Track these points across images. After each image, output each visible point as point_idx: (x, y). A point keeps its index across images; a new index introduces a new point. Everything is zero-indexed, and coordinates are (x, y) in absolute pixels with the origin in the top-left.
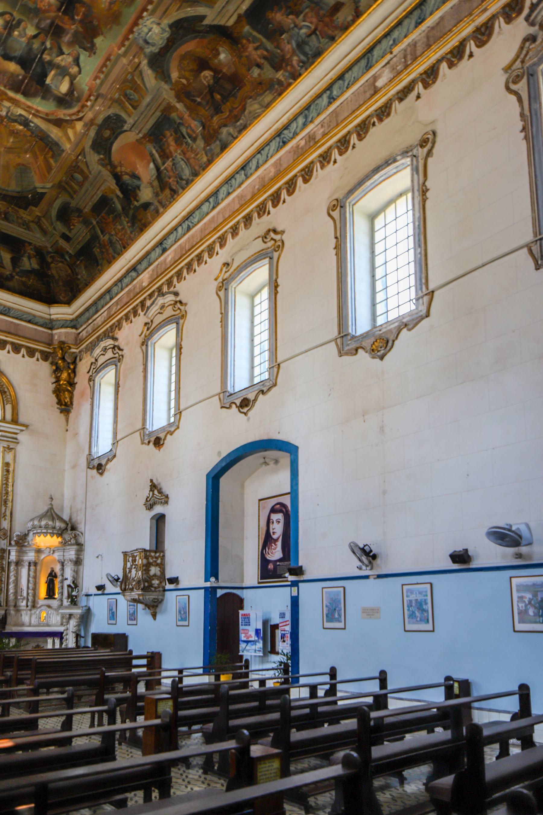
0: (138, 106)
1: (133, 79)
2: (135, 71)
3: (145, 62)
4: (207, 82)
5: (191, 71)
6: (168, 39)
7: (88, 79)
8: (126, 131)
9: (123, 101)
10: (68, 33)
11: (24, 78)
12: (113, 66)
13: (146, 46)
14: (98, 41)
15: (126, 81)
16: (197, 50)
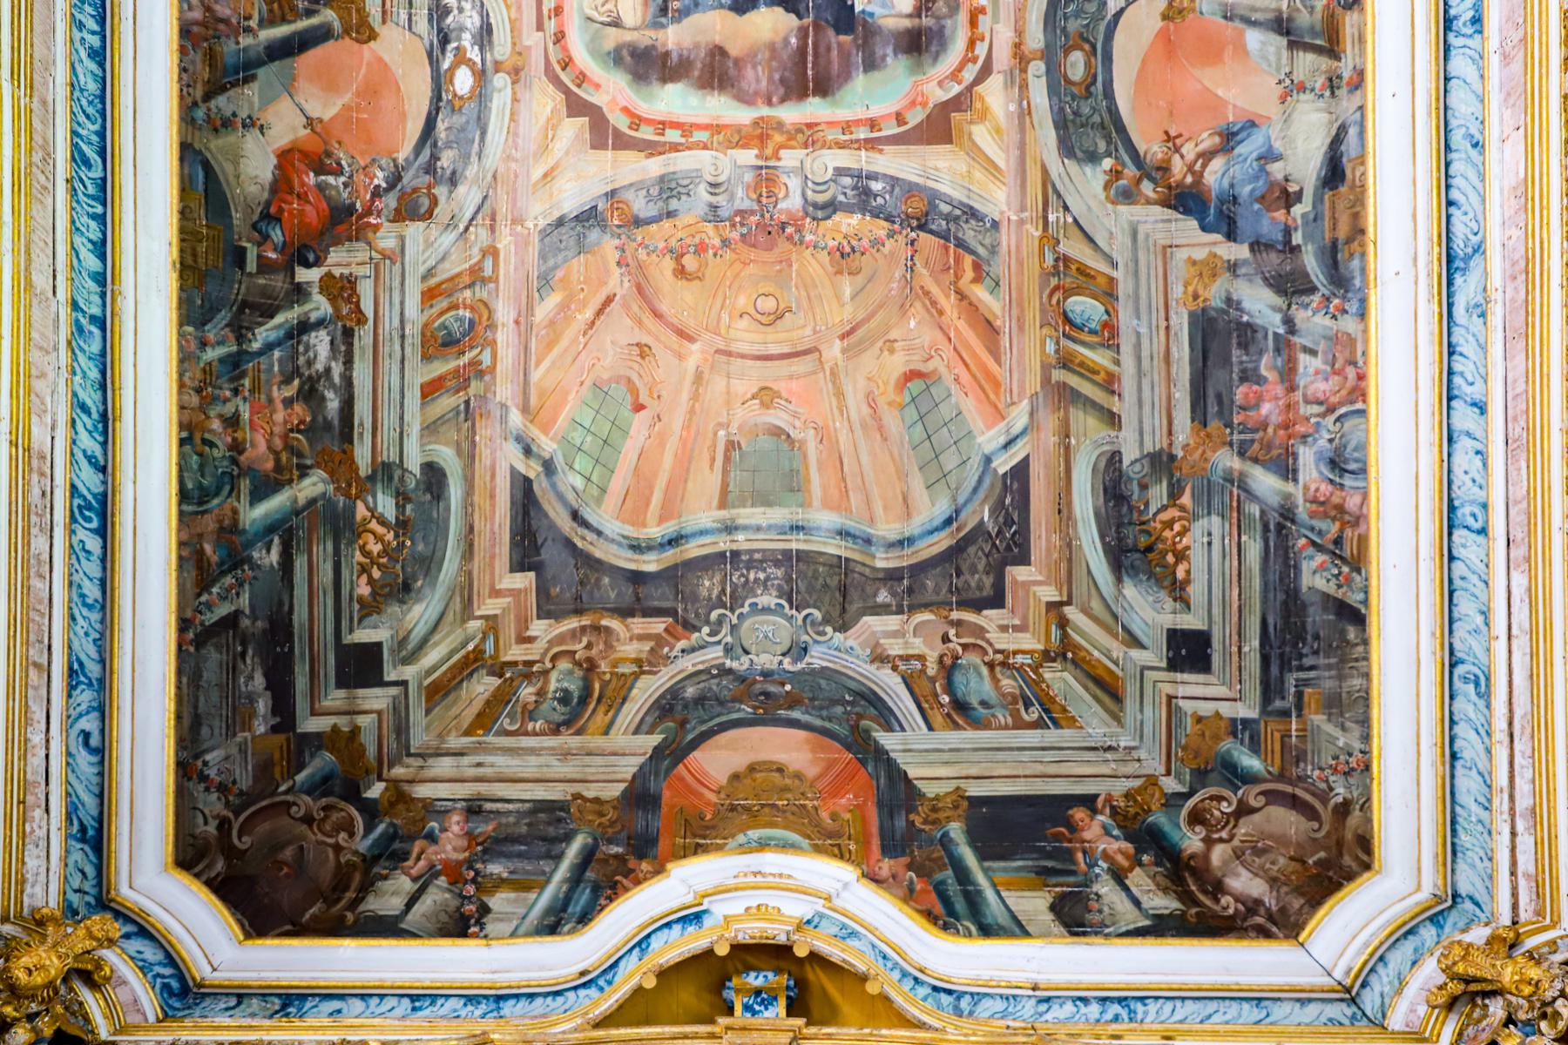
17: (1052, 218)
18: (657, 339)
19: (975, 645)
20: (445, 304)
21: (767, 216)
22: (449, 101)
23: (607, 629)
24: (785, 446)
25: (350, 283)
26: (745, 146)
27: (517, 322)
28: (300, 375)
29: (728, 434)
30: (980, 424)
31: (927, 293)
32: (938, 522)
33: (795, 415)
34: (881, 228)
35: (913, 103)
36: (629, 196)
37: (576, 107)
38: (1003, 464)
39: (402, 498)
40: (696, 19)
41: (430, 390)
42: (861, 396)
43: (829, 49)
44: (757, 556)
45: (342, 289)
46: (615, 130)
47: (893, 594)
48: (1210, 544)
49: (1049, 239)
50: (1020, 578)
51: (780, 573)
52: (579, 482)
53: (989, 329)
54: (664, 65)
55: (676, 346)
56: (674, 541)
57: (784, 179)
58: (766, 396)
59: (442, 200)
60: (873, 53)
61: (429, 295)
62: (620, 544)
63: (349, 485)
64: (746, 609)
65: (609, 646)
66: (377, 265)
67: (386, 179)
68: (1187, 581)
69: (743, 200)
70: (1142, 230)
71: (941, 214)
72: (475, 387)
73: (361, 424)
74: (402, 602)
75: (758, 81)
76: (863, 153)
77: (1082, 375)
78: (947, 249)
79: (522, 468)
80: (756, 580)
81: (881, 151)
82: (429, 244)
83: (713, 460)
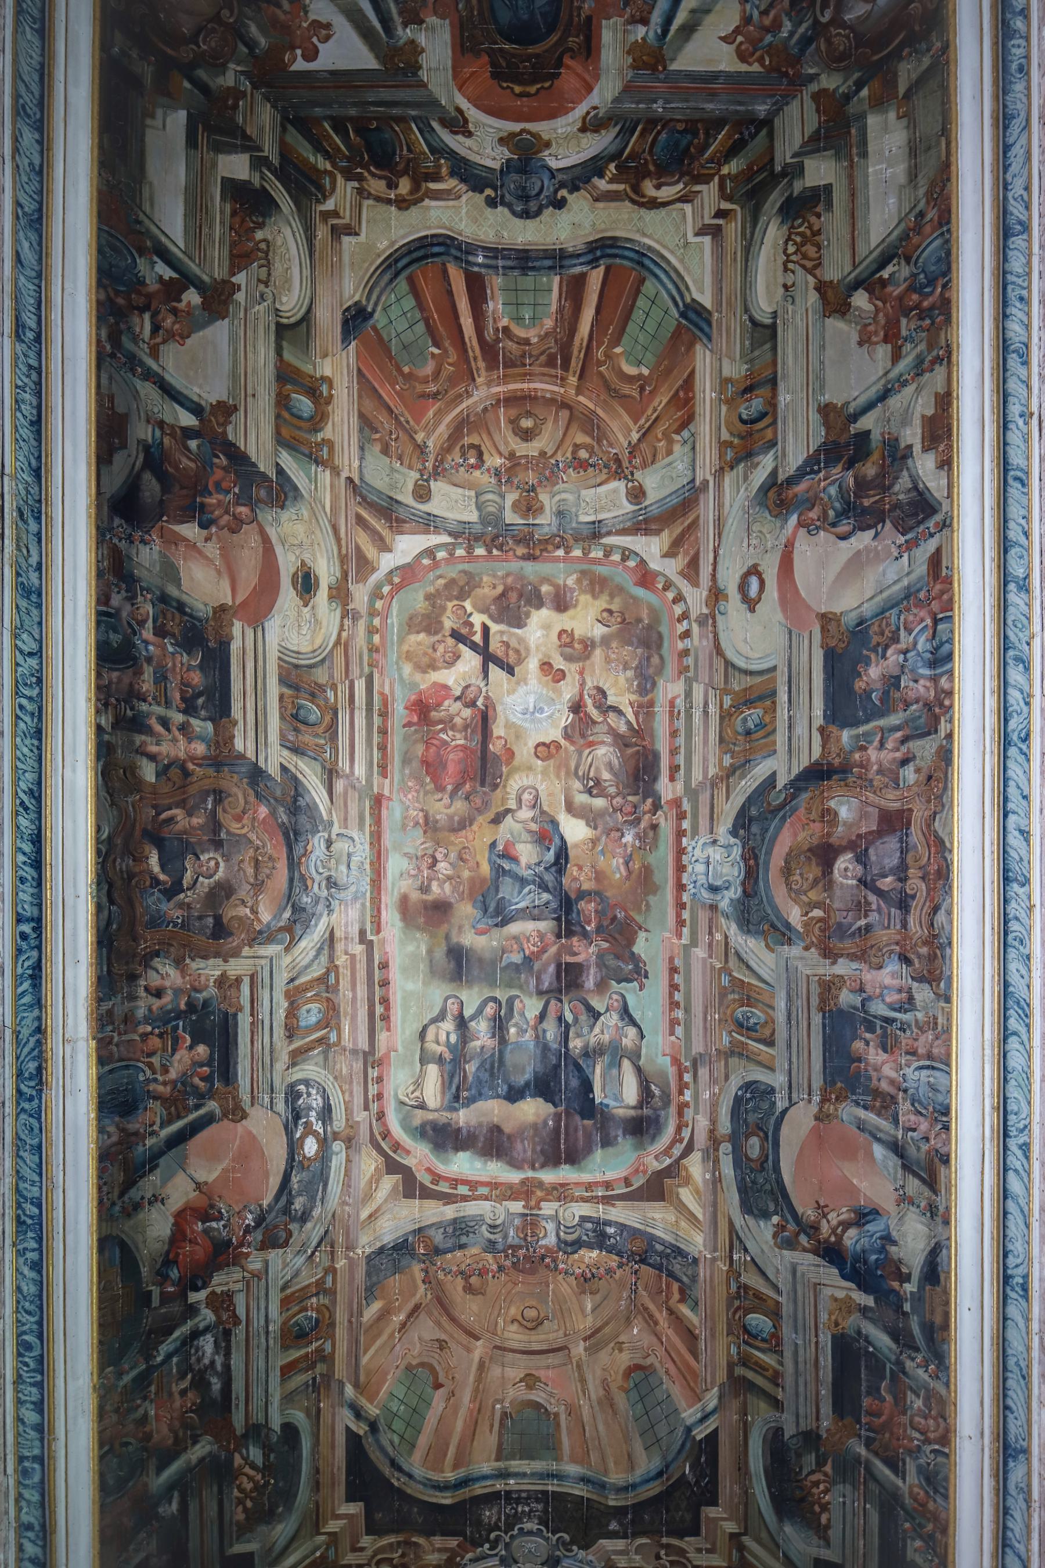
0: (773, 1033)
1: (733, 980)
2: (726, 961)
3: (733, 929)
4: (853, 878)
5: (816, 881)
7: (660, 1039)
8: (784, 1112)
10: (589, 969)
11: (557, 1117)
12: (688, 980)
14: (640, 947)
15: (723, 993)
17: (735, 1257)
18: (451, 1336)
19: (678, 1562)
20: (296, 1308)
22: (300, 1162)
23: (415, 1543)
24: (544, 1417)
25: (228, 1296)
27: (350, 1322)
28: (192, 1370)
29: (503, 1407)
30: (684, 1404)
31: (646, 1309)
32: (653, 1474)
33: (551, 1395)
34: (613, 1261)
35: (637, 1171)
36: (432, 1232)
37: (392, 1167)
38: (700, 1433)
39: (267, 1448)
40: (481, 1105)
41: (287, 1371)
42: (598, 1382)
45: (222, 1302)
47: (621, 1524)
48: (844, 1503)
49: (733, 1273)
50: (711, 1515)
52: (396, 1439)
53: (690, 1337)
55: (465, 1342)
56: (464, 1482)
58: (530, 1380)
59: (295, 1234)
61: (285, 1302)
62: (425, 1485)
63: (229, 1443)
64: (516, 1532)
65: (418, 1557)
66: (248, 1282)
67: (254, 1220)
68: (828, 1527)
70: (799, 1268)
71: (656, 1252)
72: (320, 1368)
73: (237, 1398)
74: (268, 1523)
77: (756, 1371)
78: (660, 1277)
79: (354, 1427)
80: (523, 1512)
82: (285, 1265)
83: (492, 1426)
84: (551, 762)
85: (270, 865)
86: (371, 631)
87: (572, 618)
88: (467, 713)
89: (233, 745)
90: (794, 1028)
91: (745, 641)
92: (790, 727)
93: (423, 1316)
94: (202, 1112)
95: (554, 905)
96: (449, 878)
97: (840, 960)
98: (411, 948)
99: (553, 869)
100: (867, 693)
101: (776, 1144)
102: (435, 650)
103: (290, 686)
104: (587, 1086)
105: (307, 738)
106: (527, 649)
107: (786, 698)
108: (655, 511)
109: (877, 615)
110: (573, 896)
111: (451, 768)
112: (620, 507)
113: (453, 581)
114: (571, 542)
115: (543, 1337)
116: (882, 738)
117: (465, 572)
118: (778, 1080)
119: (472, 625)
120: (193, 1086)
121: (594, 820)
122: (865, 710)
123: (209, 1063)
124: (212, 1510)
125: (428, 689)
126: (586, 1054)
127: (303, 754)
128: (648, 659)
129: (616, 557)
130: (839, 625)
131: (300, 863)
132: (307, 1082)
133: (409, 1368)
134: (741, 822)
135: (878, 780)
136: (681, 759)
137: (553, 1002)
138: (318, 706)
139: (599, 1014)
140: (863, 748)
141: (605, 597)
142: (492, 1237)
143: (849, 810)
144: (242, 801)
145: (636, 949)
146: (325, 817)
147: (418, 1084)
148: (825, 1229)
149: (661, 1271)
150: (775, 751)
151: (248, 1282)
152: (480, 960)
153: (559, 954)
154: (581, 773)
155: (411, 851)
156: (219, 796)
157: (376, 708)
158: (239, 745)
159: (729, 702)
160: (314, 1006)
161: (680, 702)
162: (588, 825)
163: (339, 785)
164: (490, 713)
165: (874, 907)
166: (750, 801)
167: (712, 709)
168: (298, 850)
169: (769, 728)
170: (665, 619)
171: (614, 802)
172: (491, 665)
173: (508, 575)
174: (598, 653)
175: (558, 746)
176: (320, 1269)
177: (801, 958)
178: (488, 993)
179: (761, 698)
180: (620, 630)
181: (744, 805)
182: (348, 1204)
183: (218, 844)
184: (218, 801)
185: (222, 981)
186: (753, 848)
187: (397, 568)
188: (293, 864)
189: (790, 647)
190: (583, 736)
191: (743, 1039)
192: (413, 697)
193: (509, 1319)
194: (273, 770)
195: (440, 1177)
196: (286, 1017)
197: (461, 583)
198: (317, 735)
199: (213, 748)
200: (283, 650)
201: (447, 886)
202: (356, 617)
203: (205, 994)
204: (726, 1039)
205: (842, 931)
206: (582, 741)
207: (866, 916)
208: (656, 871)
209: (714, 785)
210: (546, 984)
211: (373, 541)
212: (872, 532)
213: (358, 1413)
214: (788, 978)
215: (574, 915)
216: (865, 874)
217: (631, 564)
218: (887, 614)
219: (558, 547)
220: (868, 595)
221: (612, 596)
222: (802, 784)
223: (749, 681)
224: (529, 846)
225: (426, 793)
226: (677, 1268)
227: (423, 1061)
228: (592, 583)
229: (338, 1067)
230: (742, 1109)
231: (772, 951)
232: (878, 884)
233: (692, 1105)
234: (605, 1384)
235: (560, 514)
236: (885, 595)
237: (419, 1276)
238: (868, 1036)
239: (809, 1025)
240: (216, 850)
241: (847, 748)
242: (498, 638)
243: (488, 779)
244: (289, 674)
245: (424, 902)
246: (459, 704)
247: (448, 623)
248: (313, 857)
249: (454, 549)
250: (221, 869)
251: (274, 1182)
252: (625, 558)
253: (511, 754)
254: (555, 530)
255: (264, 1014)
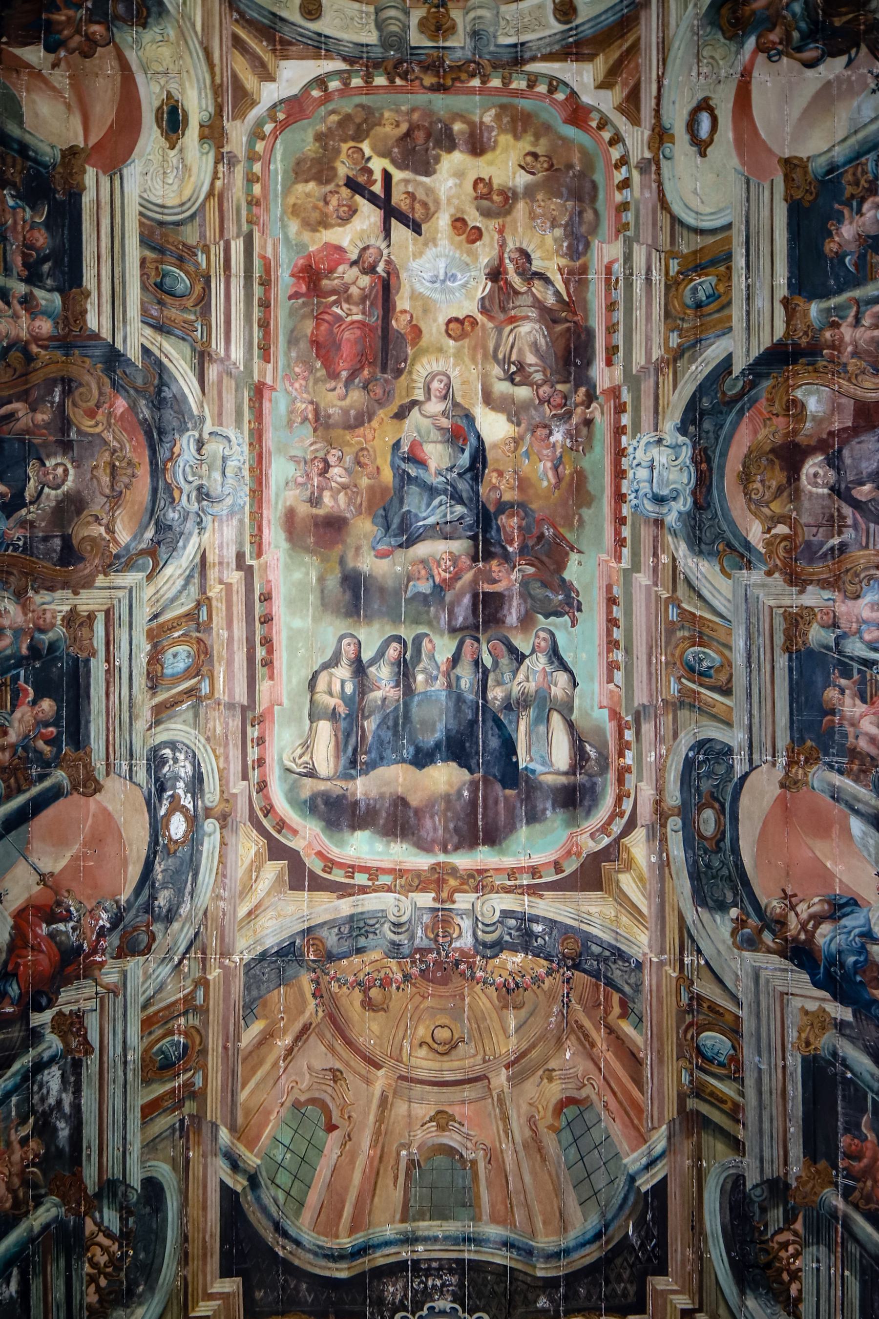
0: (730, 680)
1: (683, 612)
3: (682, 550)
5: (780, 490)
6: (693, 460)
7: (596, 687)
8: (744, 777)
9: (694, 691)
10: (511, 598)
12: (628, 613)
13: (665, 510)
14: (572, 572)
16: (760, 437)
17: (687, 960)
18: (347, 1064)
20: (159, 1032)
21: (443, 953)
26: (424, 890)
31: (581, 1027)
34: (541, 966)
36: (324, 933)
43: (496, 802)
44: (435, 1265)
46: (311, 872)
49: (685, 980)
51: (454, 1280)
54: (354, 814)
55: (364, 1072)
57: (458, 920)
59: (159, 937)
60: (534, 807)
61: (147, 1024)
66: (102, 999)
67: (109, 920)
69: (421, 938)
70: (763, 974)
71: (592, 954)
75: (435, 829)
76: (526, 898)
78: (597, 986)
81: (541, 896)
82: (147, 977)
84: (466, 342)
85: (129, 471)
86: (251, 179)
87: (490, 163)
88: (365, 281)
89: (85, 321)
90: (755, 673)
91: (695, 192)
92: (748, 299)
93: (313, 1038)
94: (47, 784)
95: (469, 520)
96: (344, 487)
97: (810, 588)
98: (298, 575)
99: (468, 476)
100: (840, 257)
101: (735, 819)
102: (327, 203)
103: (153, 249)
104: (509, 746)
105: (173, 313)
106: (437, 202)
107: (742, 262)
108: (588, 31)
109: (850, 161)
110: (492, 509)
111: (346, 350)
112: (546, 26)
113: (348, 118)
114: (489, 69)
115: (456, 1064)
116: (858, 312)
117: (362, 106)
118: (736, 738)
119: (370, 172)
120: (36, 751)
121: (517, 414)
122: (837, 279)
123: (56, 723)
124: (59, 1293)
125: (319, 251)
126: (508, 707)
127: (169, 333)
128: (581, 213)
129: (542, 88)
130: (806, 173)
131: (165, 469)
132: (173, 745)
133: (297, 1105)
134: (691, 416)
135: (853, 365)
136: (619, 339)
137: (468, 641)
138: (187, 273)
139: (524, 657)
140: (835, 325)
141: (529, 138)
142: (396, 938)
143: (819, 401)
144: (95, 392)
145: (567, 575)
146: (196, 412)
147: (307, 746)
148: (793, 924)
149: (599, 979)
150: (730, 329)
151: (102, 999)
152: (382, 590)
153: (475, 581)
154: (501, 356)
155: (299, 453)
156: (69, 385)
157: (256, 274)
158: (92, 322)
159: (676, 268)
160: (183, 650)
161: (618, 267)
162: (510, 420)
163: (212, 372)
164: (393, 281)
165: (849, 521)
166: (701, 390)
167: (657, 276)
168: (163, 453)
169: (724, 300)
170: (600, 165)
171: (541, 392)
172: (394, 222)
173: (413, 110)
174: (521, 207)
175: (474, 322)
176: (189, 981)
177: (763, 585)
178: (390, 631)
179: (714, 263)
180: (547, 179)
181: (694, 395)
182: (223, 899)
183: (66, 446)
184: (66, 393)
185: (71, 618)
186: (705, 449)
187: (282, 102)
188: (157, 470)
189: (748, 200)
190: (503, 309)
191: (694, 686)
192: (301, 262)
193: (416, 1042)
194: (133, 353)
195: (333, 862)
196: (148, 663)
197: (358, 120)
198: (185, 309)
199: (61, 326)
200: (145, 203)
201: (342, 497)
202: (232, 162)
203: (51, 635)
204: (674, 687)
205: (811, 552)
206: (502, 317)
207: (840, 533)
208: (590, 478)
209: (658, 370)
210: (461, 619)
211: (254, 67)
212: (844, 59)
213: (235, 1165)
214: (747, 610)
215: (493, 533)
216: (838, 481)
217: (560, 96)
218: (863, 160)
219: (473, 76)
220: (840, 136)
221: (537, 137)
222: (763, 369)
223: (700, 241)
224: (440, 447)
225: (316, 382)
226: (616, 975)
227: (313, 717)
228: (513, 121)
229: (210, 725)
230: (694, 774)
231: (728, 576)
232: (854, 493)
233: (634, 769)
234: (532, 1122)
235: (475, 34)
236: (860, 136)
237: (308, 988)
238: (843, 682)
239: (773, 668)
240: (65, 454)
241: (816, 325)
242: (402, 188)
243: (391, 363)
244: (152, 233)
245: (315, 517)
246: (355, 270)
247: (343, 170)
248: (181, 462)
249: (349, 78)
250: (70, 478)
251: (134, 872)
252: (552, 90)
253: (417, 332)
254: (469, 54)
255: (122, 658)
